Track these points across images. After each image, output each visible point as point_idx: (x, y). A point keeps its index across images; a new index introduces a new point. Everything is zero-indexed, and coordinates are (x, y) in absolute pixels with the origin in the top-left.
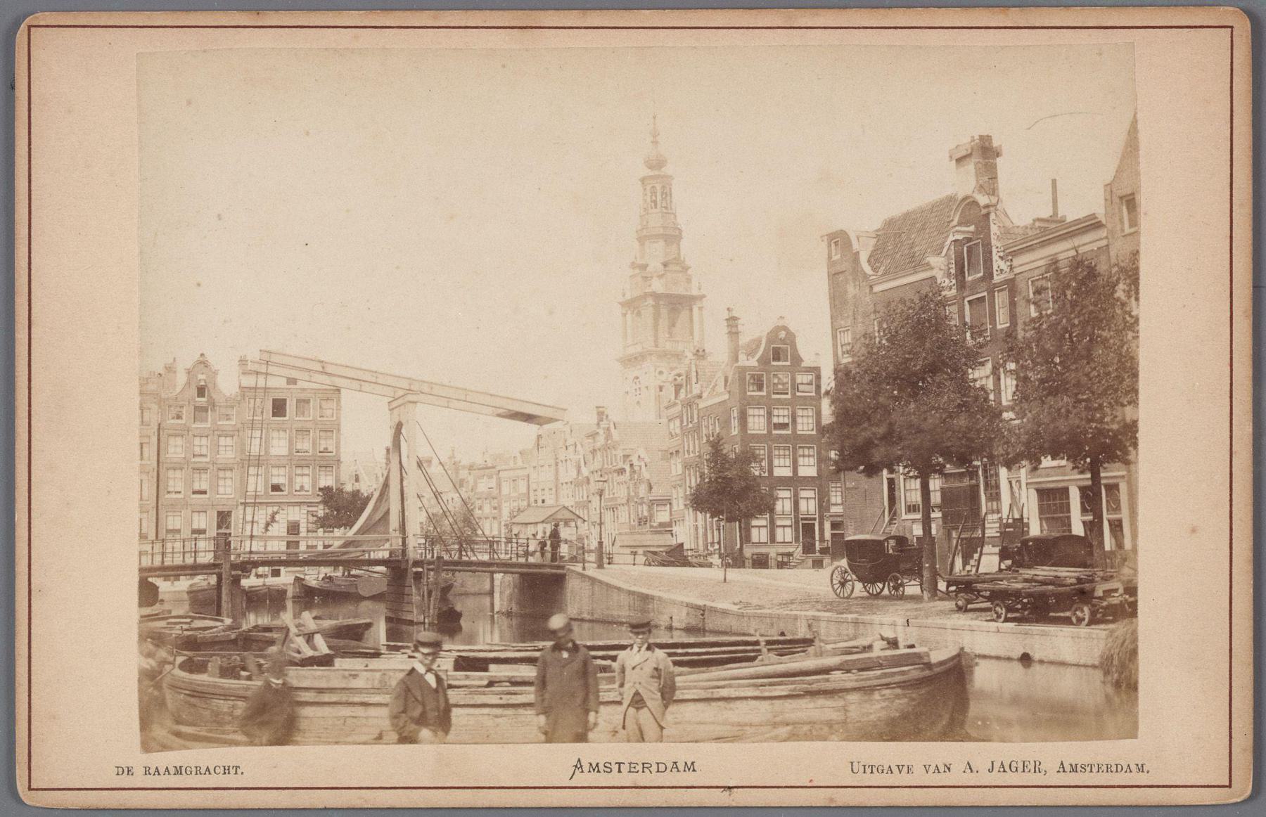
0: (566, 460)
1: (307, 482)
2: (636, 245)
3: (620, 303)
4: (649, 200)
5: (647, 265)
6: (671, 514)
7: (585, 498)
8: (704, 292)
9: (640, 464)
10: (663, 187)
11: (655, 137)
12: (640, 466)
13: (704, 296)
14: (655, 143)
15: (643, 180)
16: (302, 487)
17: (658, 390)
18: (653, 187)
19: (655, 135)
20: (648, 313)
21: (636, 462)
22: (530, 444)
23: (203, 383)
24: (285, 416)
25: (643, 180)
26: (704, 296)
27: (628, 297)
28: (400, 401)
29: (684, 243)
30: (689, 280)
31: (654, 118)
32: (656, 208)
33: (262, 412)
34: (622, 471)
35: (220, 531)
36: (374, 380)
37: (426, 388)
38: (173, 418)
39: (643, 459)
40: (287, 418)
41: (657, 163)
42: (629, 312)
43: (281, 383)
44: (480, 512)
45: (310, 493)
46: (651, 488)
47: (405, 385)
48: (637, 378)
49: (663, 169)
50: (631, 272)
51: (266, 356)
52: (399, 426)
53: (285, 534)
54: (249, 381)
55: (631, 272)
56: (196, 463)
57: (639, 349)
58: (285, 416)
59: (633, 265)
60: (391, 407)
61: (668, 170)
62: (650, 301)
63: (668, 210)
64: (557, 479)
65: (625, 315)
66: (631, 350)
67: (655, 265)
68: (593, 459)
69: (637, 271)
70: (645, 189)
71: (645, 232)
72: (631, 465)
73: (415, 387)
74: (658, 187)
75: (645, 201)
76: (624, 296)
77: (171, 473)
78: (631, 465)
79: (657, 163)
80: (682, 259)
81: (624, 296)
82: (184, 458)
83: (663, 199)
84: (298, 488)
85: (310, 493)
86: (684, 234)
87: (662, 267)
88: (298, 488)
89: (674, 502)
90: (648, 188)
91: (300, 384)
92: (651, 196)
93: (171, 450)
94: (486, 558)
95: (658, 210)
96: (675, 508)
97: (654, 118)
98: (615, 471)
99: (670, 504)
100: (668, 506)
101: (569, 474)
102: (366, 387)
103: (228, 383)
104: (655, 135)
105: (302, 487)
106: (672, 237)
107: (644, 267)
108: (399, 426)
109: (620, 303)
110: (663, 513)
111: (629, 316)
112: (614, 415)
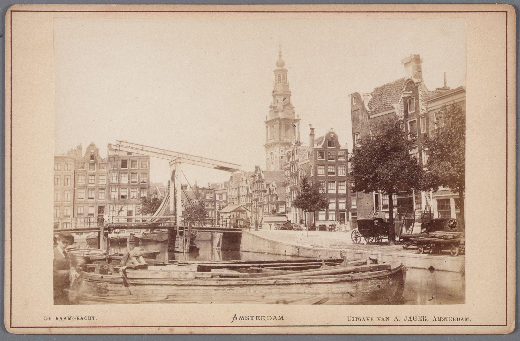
0: (243, 187)
1: (135, 195)
3: (265, 122)
5: (276, 107)
6: (286, 209)
7: (250, 202)
8: (300, 118)
9: (273, 188)
11: (280, 53)
12: (273, 189)
13: (300, 119)
14: (280, 56)
15: (275, 71)
16: (134, 197)
17: (281, 157)
20: (277, 126)
21: (271, 187)
22: (228, 179)
23: (93, 154)
24: (127, 167)
25: (275, 71)
26: (300, 119)
27: (268, 120)
28: (174, 162)
29: (291, 97)
30: (294, 113)
32: (280, 83)
33: (117, 166)
34: (266, 191)
35: (100, 214)
36: (163, 153)
37: (185, 157)
38: (80, 168)
39: (274, 186)
40: (127, 168)
41: (281, 64)
42: (269, 126)
43: (126, 154)
44: (207, 207)
45: (137, 199)
46: (277, 198)
47: (176, 155)
48: (272, 153)
49: (283, 67)
50: (270, 109)
51: (119, 143)
52: (174, 172)
53: (127, 216)
54: (112, 153)
55: (270, 109)
56: (90, 186)
57: (273, 141)
58: (127, 167)
59: (271, 107)
60: (171, 164)
61: (285, 67)
62: (278, 122)
63: (286, 85)
64: (239, 194)
65: (267, 127)
66: (270, 142)
67: (280, 106)
68: (254, 186)
69: (272, 109)
70: (276, 76)
71: (275, 93)
72: (270, 189)
73: (181, 156)
75: (276, 80)
76: (267, 119)
77: (80, 191)
78: (270, 189)
79: (281, 64)
80: (291, 104)
81: (267, 119)
82: (85, 184)
83: (283, 79)
84: (132, 197)
85: (137, 199)
86: (292, 94)
87: (282, 108)
88: (132, 197)
89: (287, 204)
90: (277, 74)
91: (133, 155)
93: (80, 181)
94: (209, 226)
95: (281, 84)
96: (287, 206)
97: (280, 45)
98: (263, 191)
99: (285, 204)
100: (285, 205)
101: (243, 192)
102: (161, 156)
103: (103, 154)
104: (280, 53)
105: (134, 197)
106: (286, 95)
107: (276, 107)
108: (174, 172)
109: (265, 122)
110: (282, 208)
111: (269, 128)
112: (263, 168)
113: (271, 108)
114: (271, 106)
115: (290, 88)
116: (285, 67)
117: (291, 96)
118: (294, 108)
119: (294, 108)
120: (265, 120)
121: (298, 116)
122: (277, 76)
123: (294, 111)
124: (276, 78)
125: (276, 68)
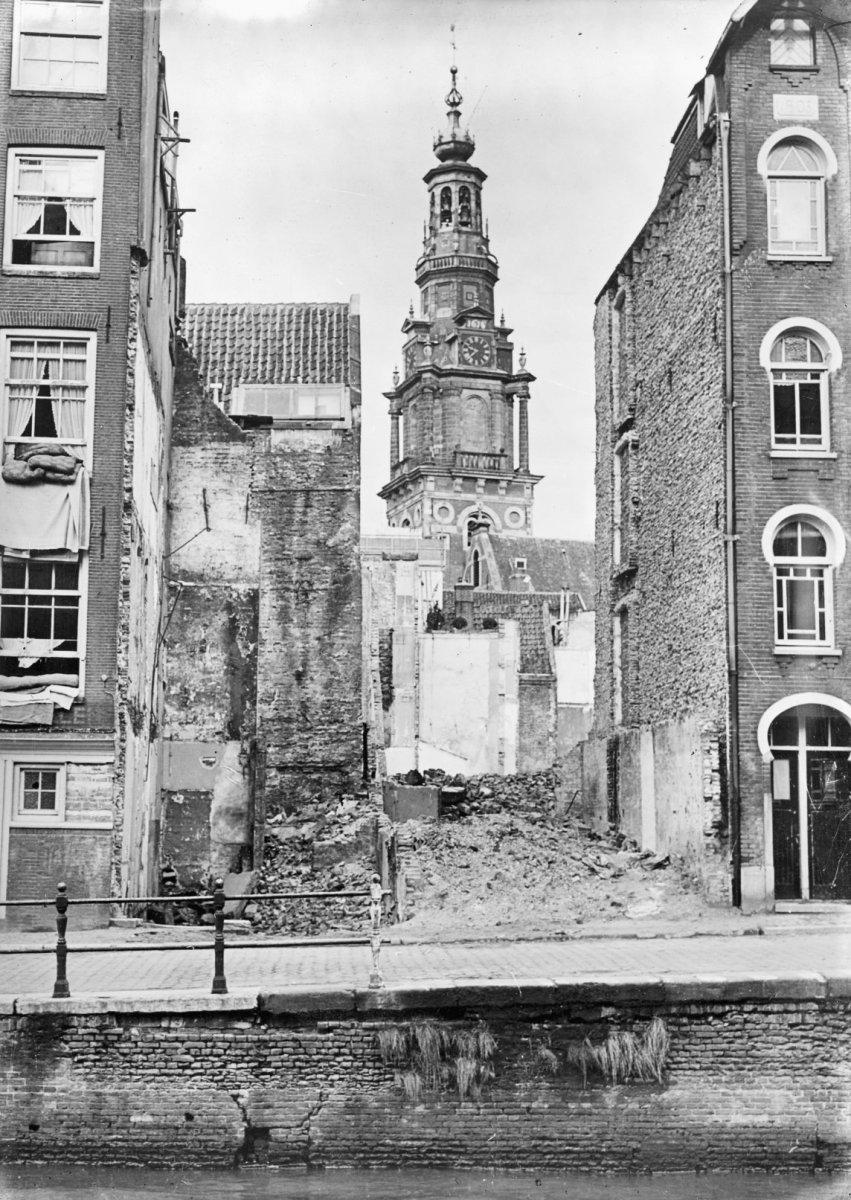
2: (417, 290)
4: (438, 210)
8: (529, 369)
26: (530, 378)
31: (454, 72)
41: (456, 153)
50: (405, 338)
55: (405, 338)
59: (411, 326)
65: (395, 414)
71: (428, 267)
74: (454, 188)
79: (456, 153)
86: (500, 274)
90: (438, 191)
92: (442, 207)
97: (454, 72)
113: (407, 332)
114: (407, 323)
115: (493, 248)
117: (497, 284)
118: (511, 331)
119: (511, 331)
121: (522, 365)
122: (438, 200)
123: (511, 344)
124: (433, 204)
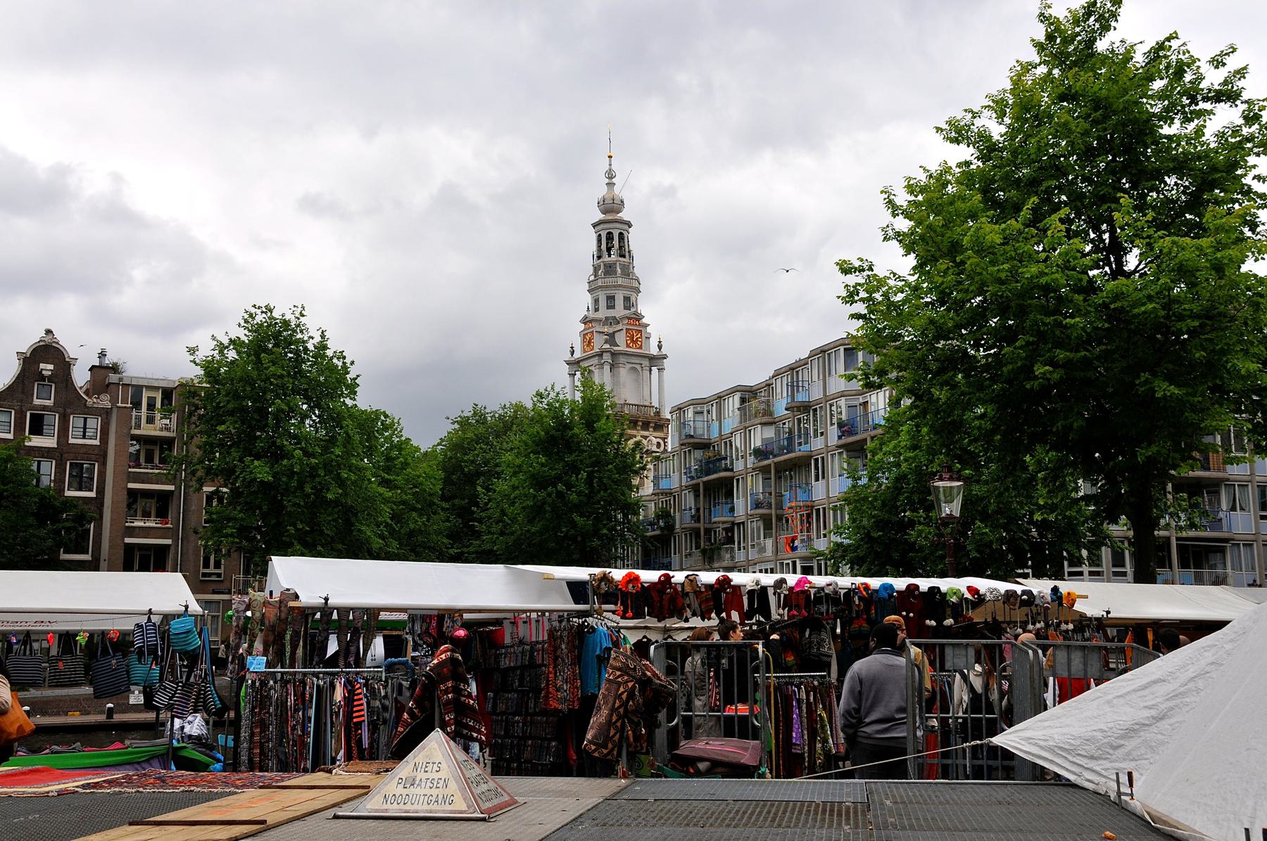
8: (664, 351)
10: (621, 234)
13: (665, 357)
18: (610, 233)
19: (610, 175)
26: (665, 357)
27: (578, 355)
31: (610, 157)
41: (611, 206)
76: (572, 355)
79: (611, 206)
81: (572, 353)
97: (610, 157)
104: (610, 175)
109: (568, 363)
113: (585, 323)
114: (586, 317)
116: (624, 215)
120: (568, 357)
123: (650, 334)
125: (600, 216)
